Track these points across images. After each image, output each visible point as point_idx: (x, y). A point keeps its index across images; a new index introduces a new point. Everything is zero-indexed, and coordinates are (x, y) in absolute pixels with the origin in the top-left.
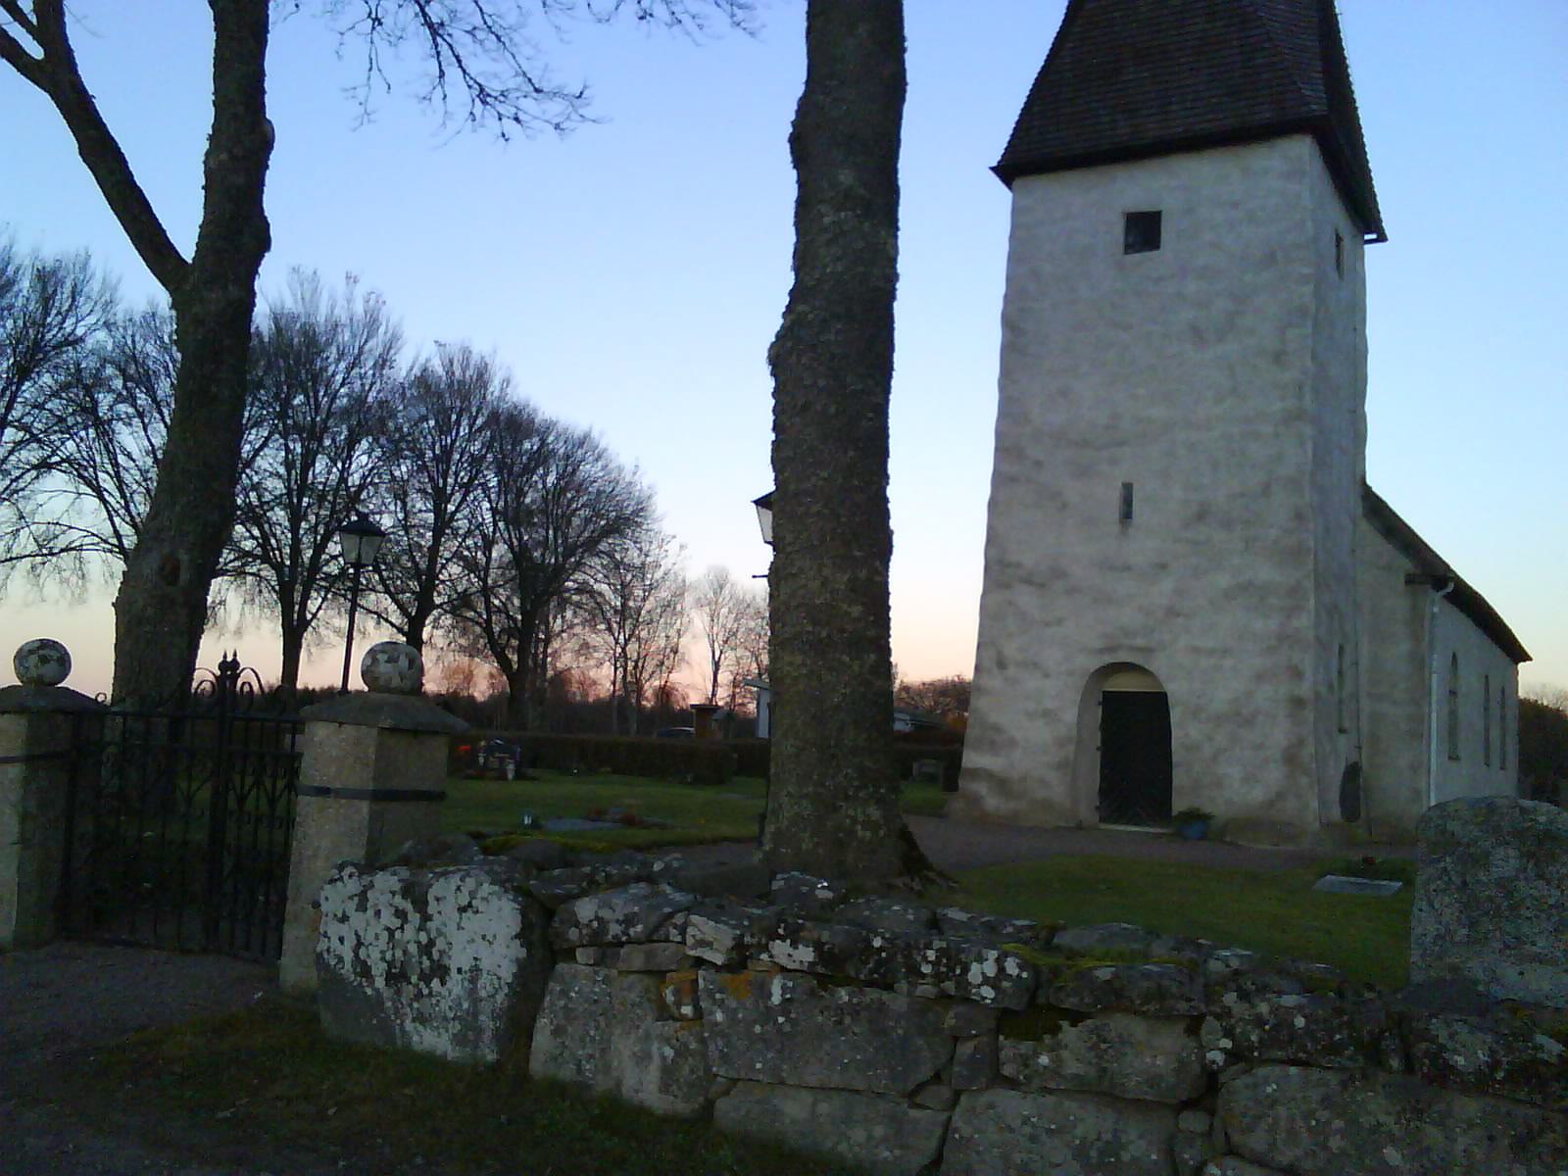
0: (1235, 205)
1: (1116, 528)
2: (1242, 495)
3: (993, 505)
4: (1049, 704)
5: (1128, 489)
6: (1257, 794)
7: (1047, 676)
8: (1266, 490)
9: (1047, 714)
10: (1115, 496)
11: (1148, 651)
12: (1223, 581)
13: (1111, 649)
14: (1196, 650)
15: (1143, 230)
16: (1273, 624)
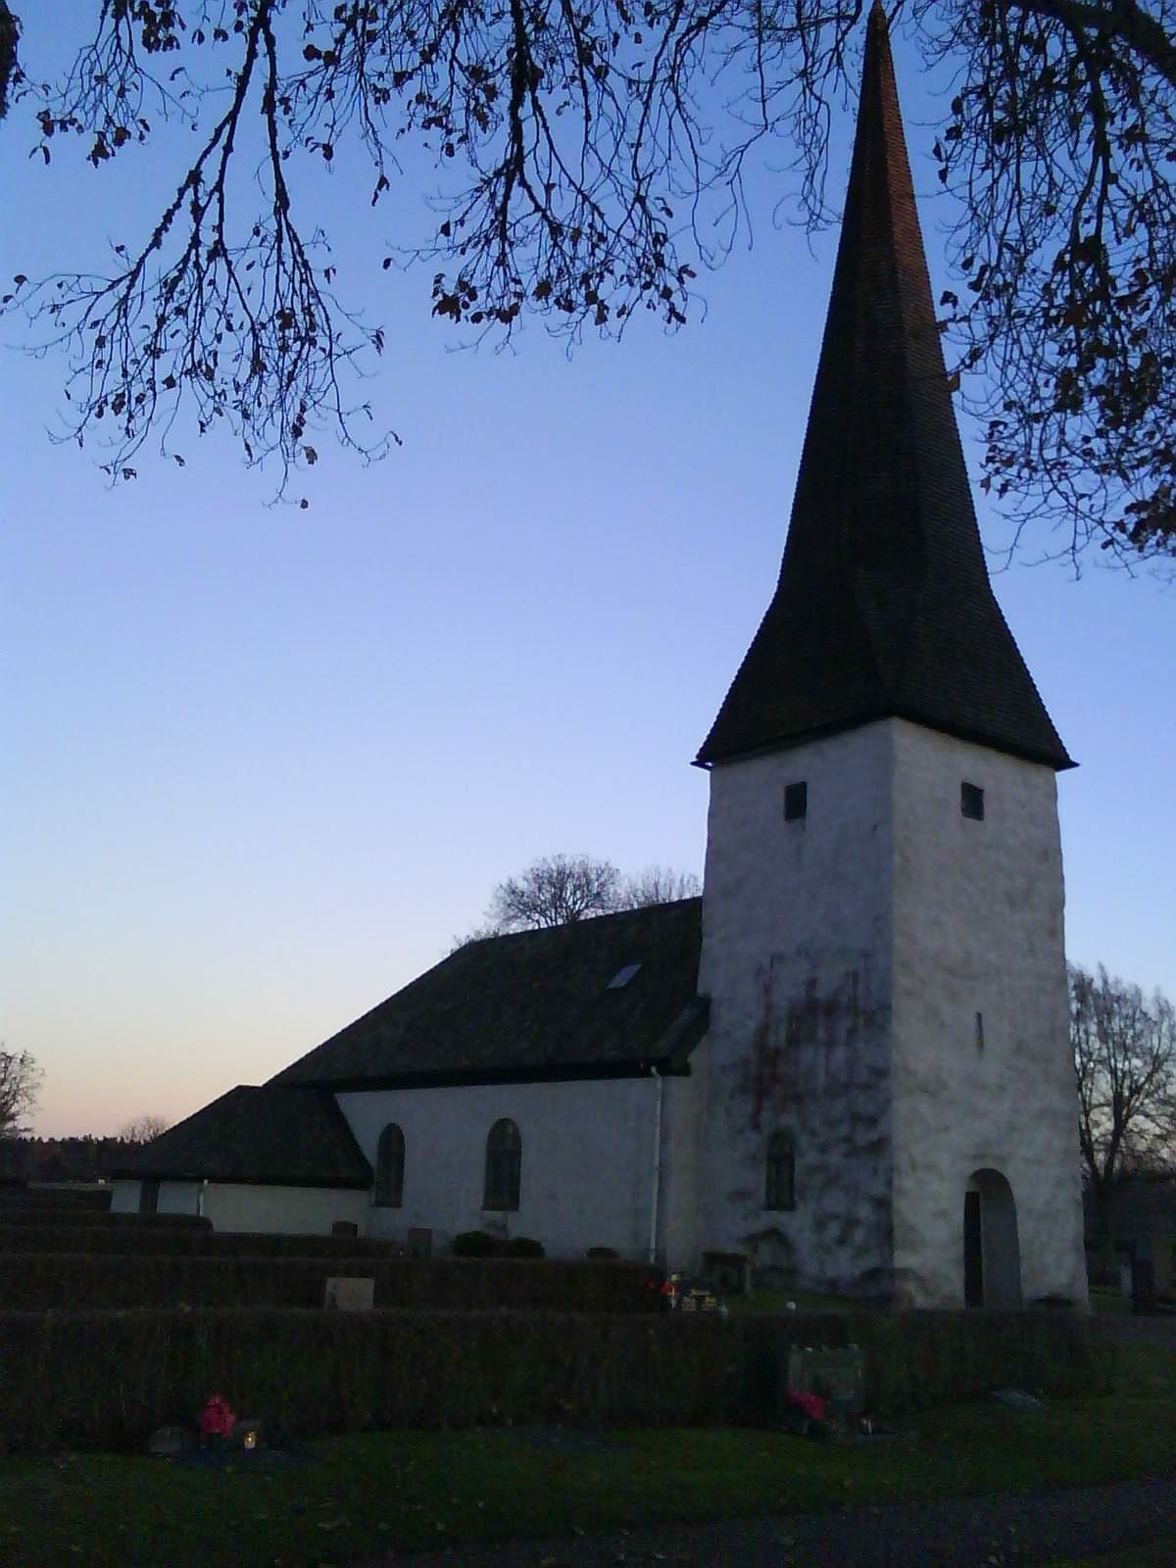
5: (979, 1016)
9: (943, 1214)
15: (973, 801)
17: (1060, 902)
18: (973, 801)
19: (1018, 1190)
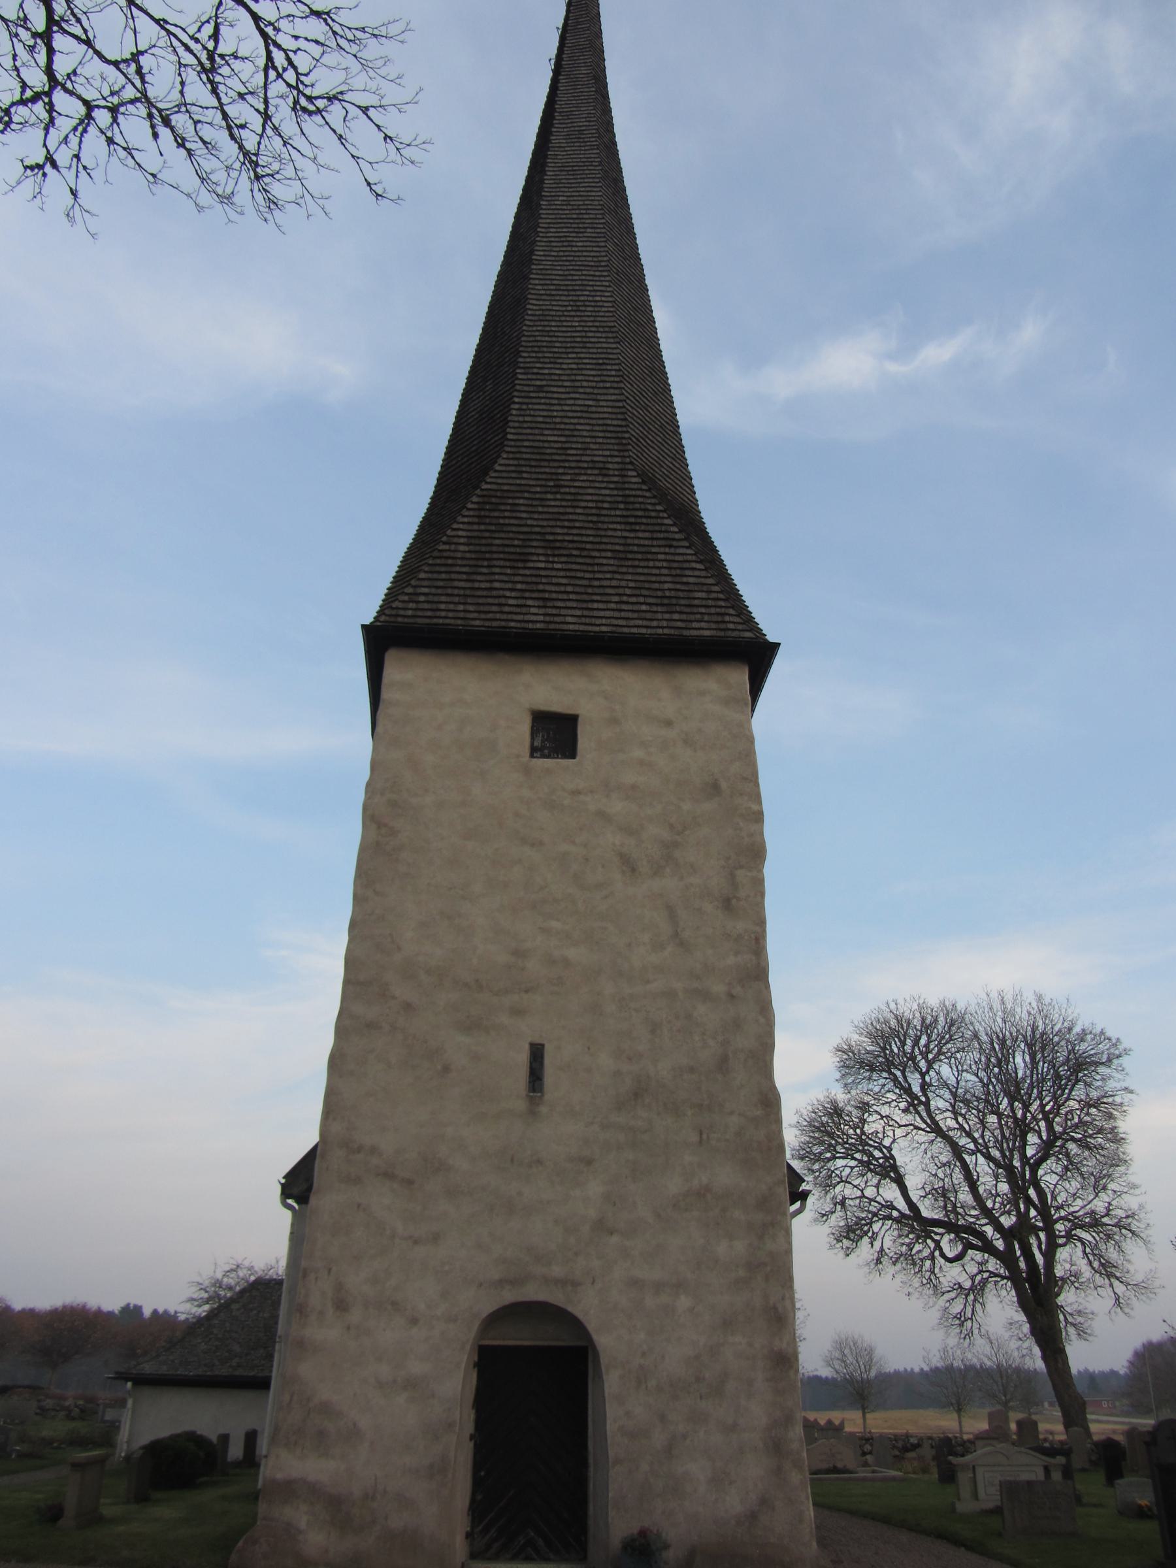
0: (669, 723)
1: (521, 1105)
2: (692, 1070)
3: (336, 1062)
4: (417, 1368)
6: (734, 1503)
7: (414, 1321)
8: (723, 1064)
10: (523, 1058)
11: (569, 1283)
12: (674, 1185)
13: (515, 1282)
14: (635, 1283)
15: (556, 734)
16: (740, 1246)
17: (756, 853)
18: (556, 734)
19: (604, 1341)
